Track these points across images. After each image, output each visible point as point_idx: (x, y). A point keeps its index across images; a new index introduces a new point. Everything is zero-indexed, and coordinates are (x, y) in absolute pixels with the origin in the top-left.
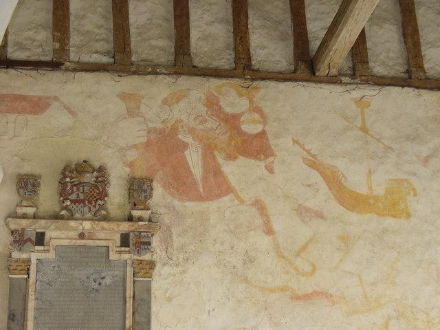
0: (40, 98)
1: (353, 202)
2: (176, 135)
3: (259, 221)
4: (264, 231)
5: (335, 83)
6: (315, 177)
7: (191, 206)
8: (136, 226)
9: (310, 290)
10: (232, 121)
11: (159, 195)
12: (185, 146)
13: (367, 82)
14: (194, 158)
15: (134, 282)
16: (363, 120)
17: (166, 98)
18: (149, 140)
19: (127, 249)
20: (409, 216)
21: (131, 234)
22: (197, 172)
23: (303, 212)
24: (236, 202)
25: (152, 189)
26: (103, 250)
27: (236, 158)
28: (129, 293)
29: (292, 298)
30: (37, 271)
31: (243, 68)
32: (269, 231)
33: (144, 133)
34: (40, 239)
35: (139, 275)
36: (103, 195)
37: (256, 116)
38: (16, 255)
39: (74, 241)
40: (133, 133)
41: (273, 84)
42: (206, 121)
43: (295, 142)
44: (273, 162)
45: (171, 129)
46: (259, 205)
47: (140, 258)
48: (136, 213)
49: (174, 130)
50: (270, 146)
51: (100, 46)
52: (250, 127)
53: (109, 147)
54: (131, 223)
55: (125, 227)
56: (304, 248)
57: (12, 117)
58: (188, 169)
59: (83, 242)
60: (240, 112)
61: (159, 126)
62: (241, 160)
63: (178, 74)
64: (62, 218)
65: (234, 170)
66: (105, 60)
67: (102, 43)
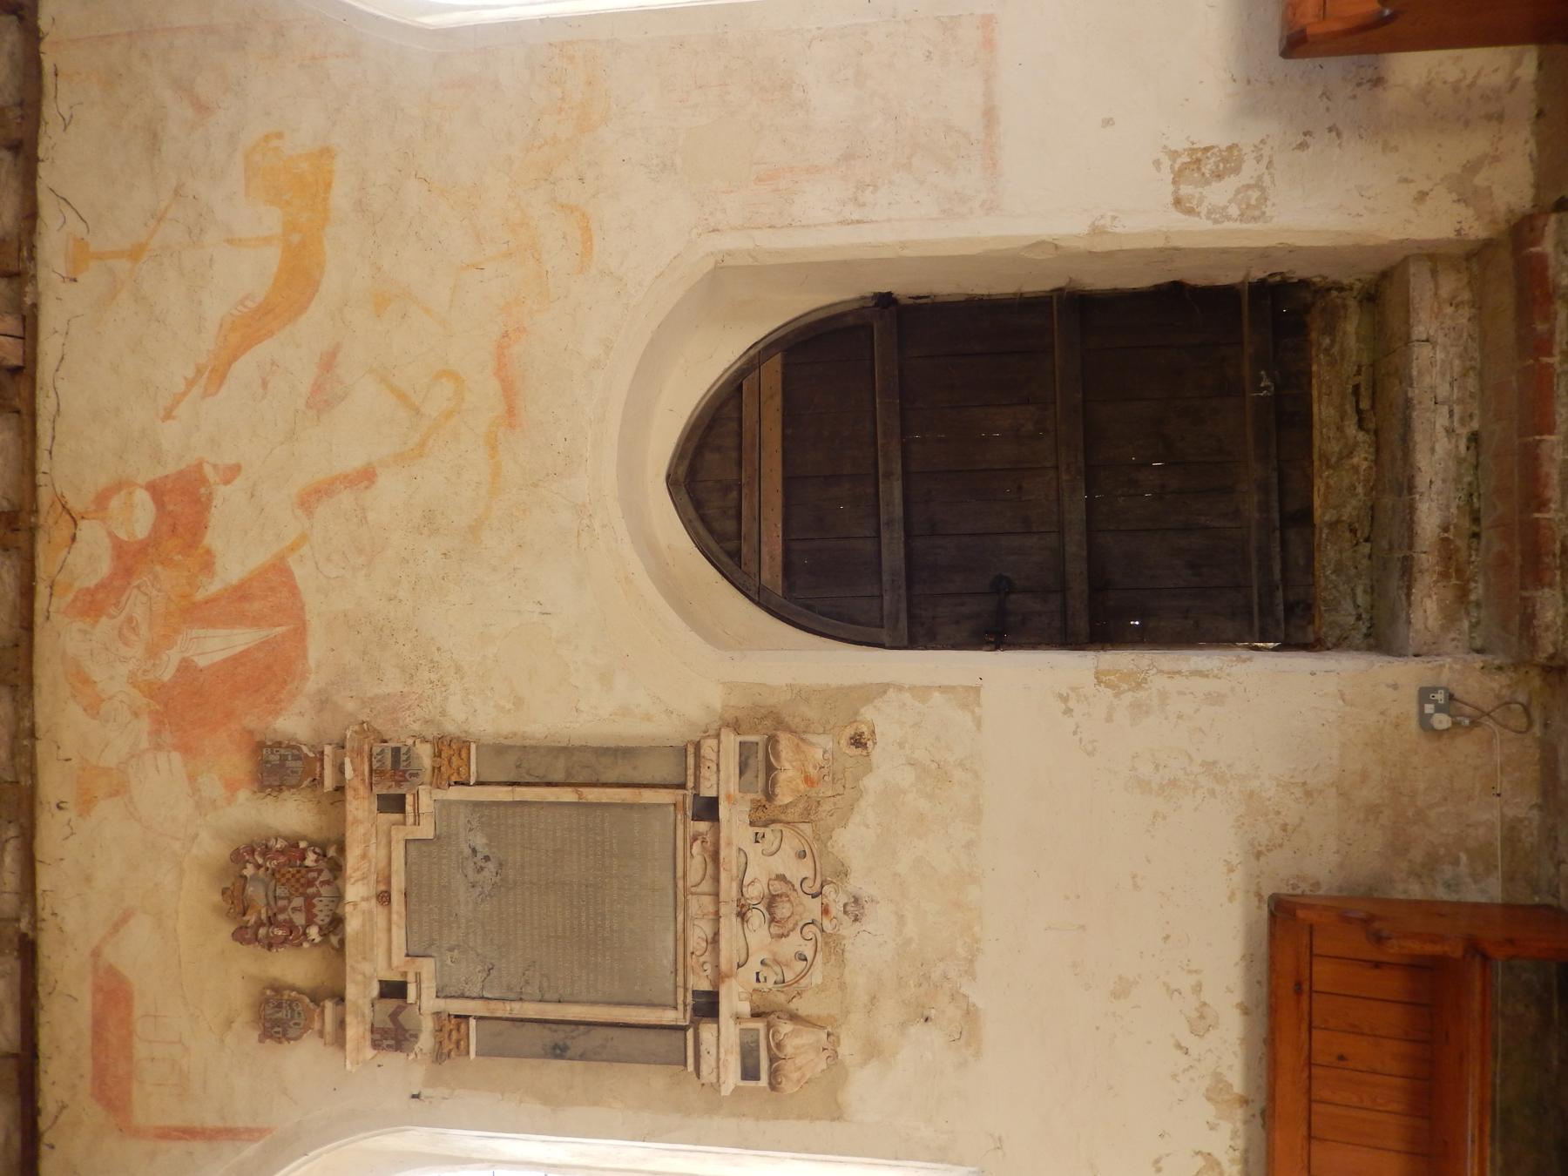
0: (97, 989)
1: (298, 279)
2: (163, 685)
3: (346, 499)
5: (35, 318)
6: (245, 367)
8: (357, 783)
9: (494, 385)
10: (130, 560)
11: (293, 724)
12: (186, 666)
13: (32, 248)
14: (215, 646)
15: (479, 783)
16: (118, 255)
18: (176, 748)
19: (409, 799)
20: (326, 152)
21: (376, 790)
22: (242, 639)
23: (324, 398)
24: (305, 550)
25: (279, 744)
26: (413, 852)
27: (208, 552)
29: (512, 426)
30: (462, 996)
32: (367, 476)
33: (162, 757)
34: (394, 990)
37: (115, 503)
38: (426, 1041)
39: (395, 917)
41: (43, 464)
42: (130, 619)
43: (168, 415)
44: (215, 466)
45: (152, 697)
46: (311, 498)
49: (154, 691)
50: (181, 473)
52: (140, 518)
53: (197, 835)
54: (349, 794)
55: (360, 807)
56: (402, 397)
57: (141, 1050)
58: (237, 660)
59: (397, 898)
60: (107, 540)
61: (145, 724)
62: (213, 539)
63: (30, 681)
64: (342, 942)
65: (235, 555)
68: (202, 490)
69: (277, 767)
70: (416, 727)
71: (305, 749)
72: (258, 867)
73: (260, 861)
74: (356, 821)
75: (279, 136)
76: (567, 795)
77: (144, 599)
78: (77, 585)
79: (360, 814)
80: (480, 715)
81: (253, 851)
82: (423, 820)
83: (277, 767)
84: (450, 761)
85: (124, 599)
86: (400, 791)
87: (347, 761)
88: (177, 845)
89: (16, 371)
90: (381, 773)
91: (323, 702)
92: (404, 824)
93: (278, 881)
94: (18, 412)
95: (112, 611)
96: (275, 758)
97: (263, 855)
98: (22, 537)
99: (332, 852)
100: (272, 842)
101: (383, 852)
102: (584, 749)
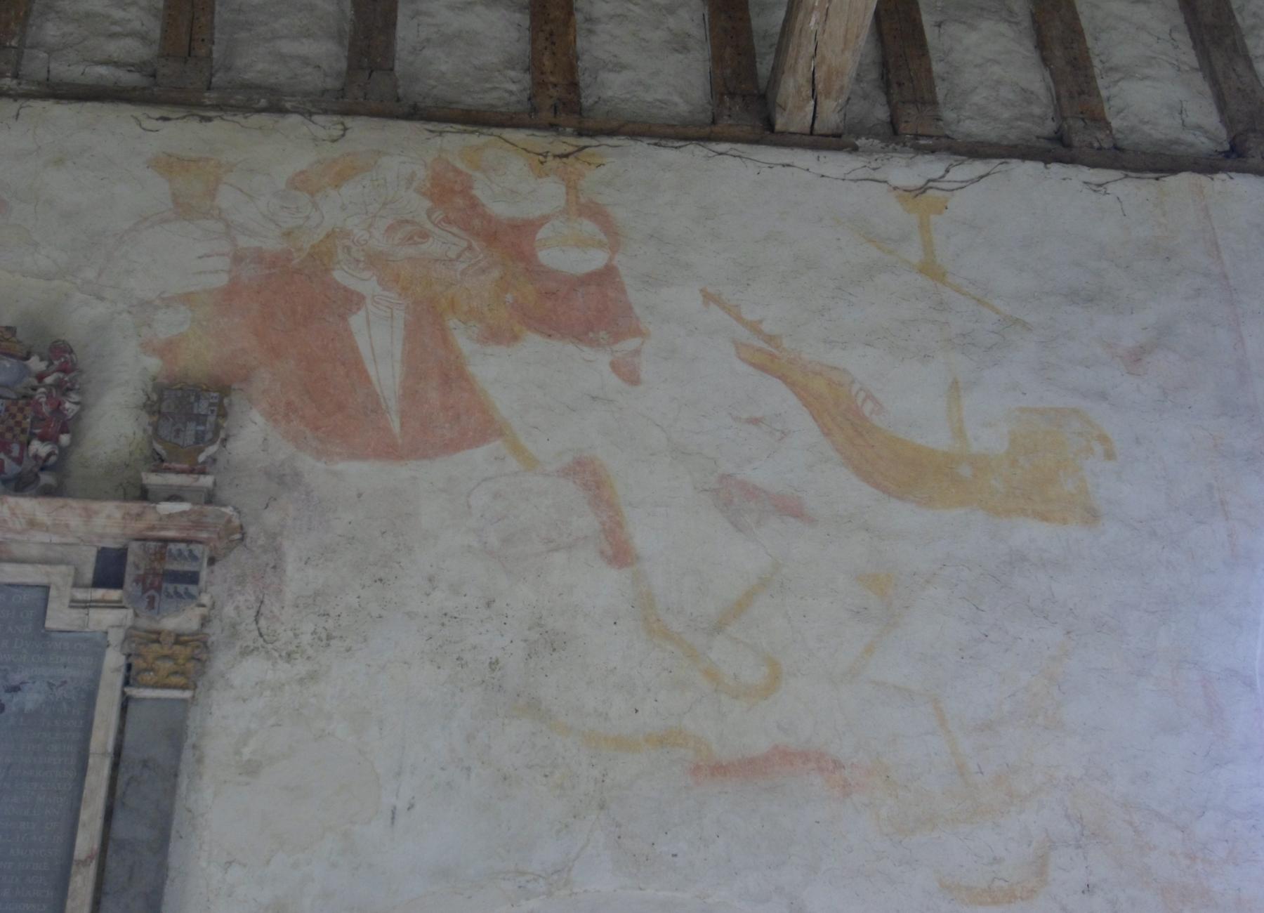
1: (907, 472)
4: (602, 553)
5: (839, 148)
6: (777, 398)
7: (360, 473)
8: (150, 518)
10: (510, 241)
11: (253, 435)
12: (352, 300)
14: (379, 342)
17: (302, 172)
19: (114, 594)
20: (1092, 516)
21: (134, 547)
23: (735, 499)
25: (223, 414)
27: (515, 338)
28: (103, 737)
29: (696, 770)
31: (558, 102)
32: (620, 553)
35: (149, 677)
36: (60, 425)
37: (589, 227)
40: (187, 262)
41: (641, 148)
42: (425, 235)
44: (637, 352)
46: (589, 477)
47: (155, 626)
48: (153, 480)
51: (114, 48)
52: (567, 254)
53: (101, 298)
54: (135, 507)
55: (109, 521)
61: (272, 243)
62: (534, 344)
65: (506, 373)
66: (129, 78)
67: (130, 43)
68: (602, 334)
69: (188, 413)
70: (229, 610)
71: (212, 450)
72: (41, 377)
73: (49, 380)
74: (89, 515)
75: (1109, 455)
76: (87, 841)
77: (452, 255)
78: (478, 175)
79: (99, 522)
80: (238, 707)
81: (64, 370)
82: (76, 614)
83: (188, 413)
84: (165, 657)
85: (455, 230)
86: (128, 579)
87: (185, 506)
88: (90, 274)
89: (769, 125)
90: (161, 555)
91: (284, 480)
92: (76, 585)
93: (15, 402)
94: (714, 122)
95: (438, 215)
96: (202, 407)
97: (58, 385)
98: (546, 116)
99: (46, 479)
100: (74, 397)
101: (35, 551)
102: (162, 870)
